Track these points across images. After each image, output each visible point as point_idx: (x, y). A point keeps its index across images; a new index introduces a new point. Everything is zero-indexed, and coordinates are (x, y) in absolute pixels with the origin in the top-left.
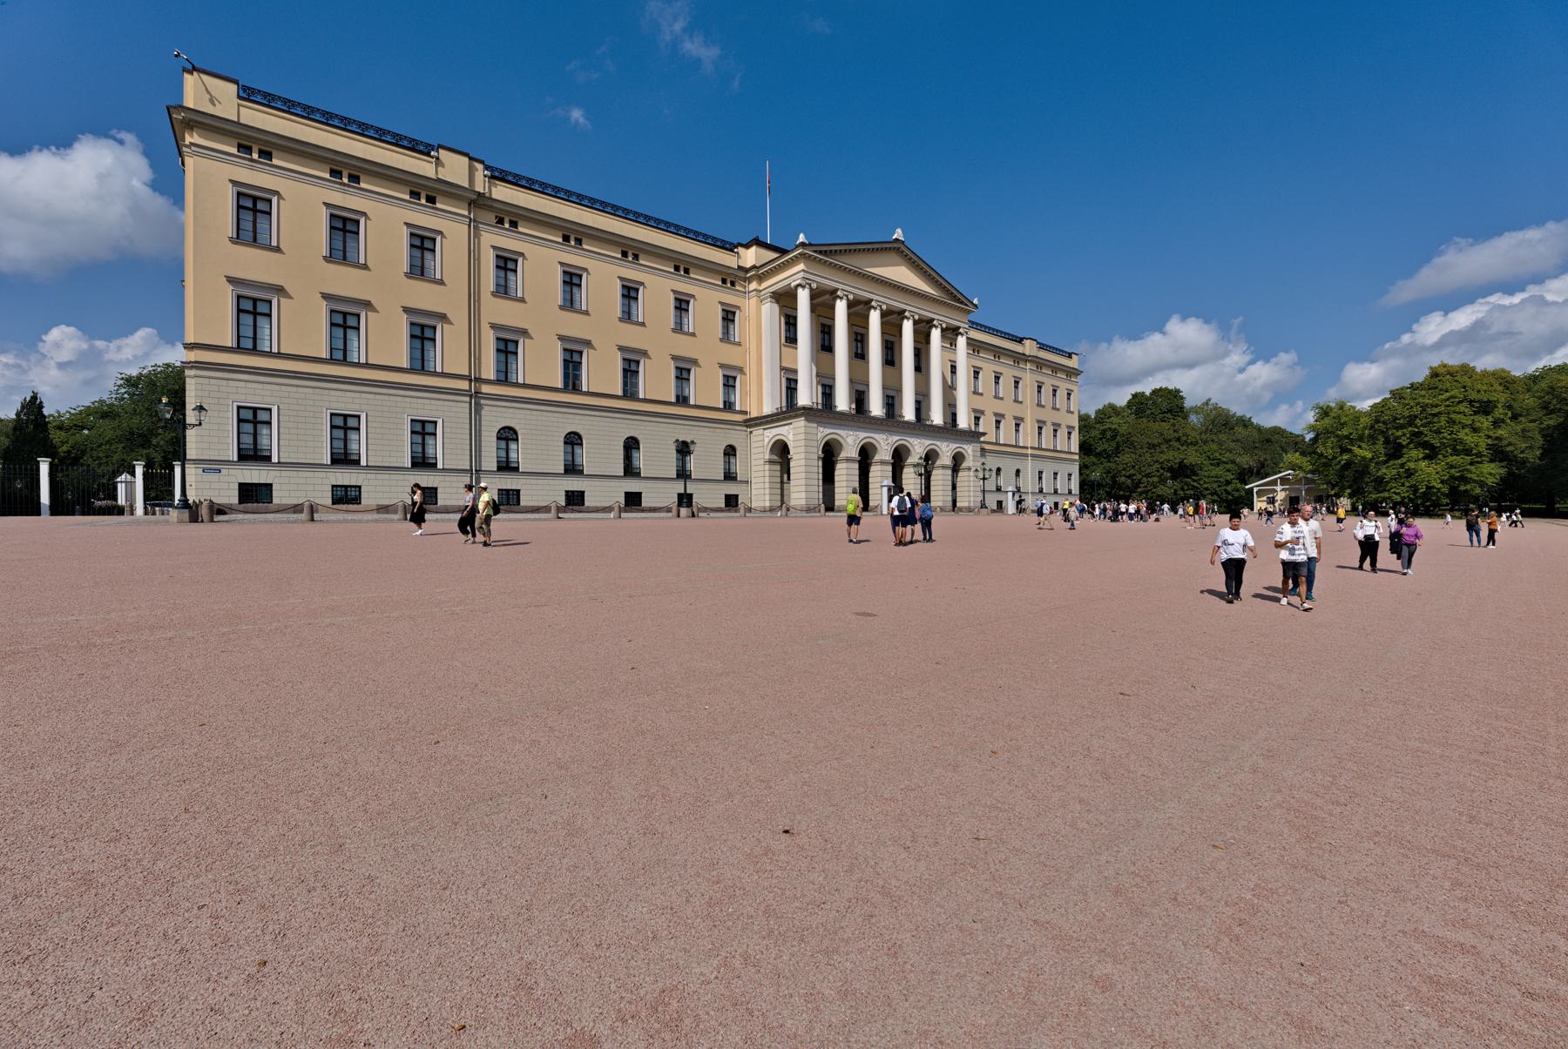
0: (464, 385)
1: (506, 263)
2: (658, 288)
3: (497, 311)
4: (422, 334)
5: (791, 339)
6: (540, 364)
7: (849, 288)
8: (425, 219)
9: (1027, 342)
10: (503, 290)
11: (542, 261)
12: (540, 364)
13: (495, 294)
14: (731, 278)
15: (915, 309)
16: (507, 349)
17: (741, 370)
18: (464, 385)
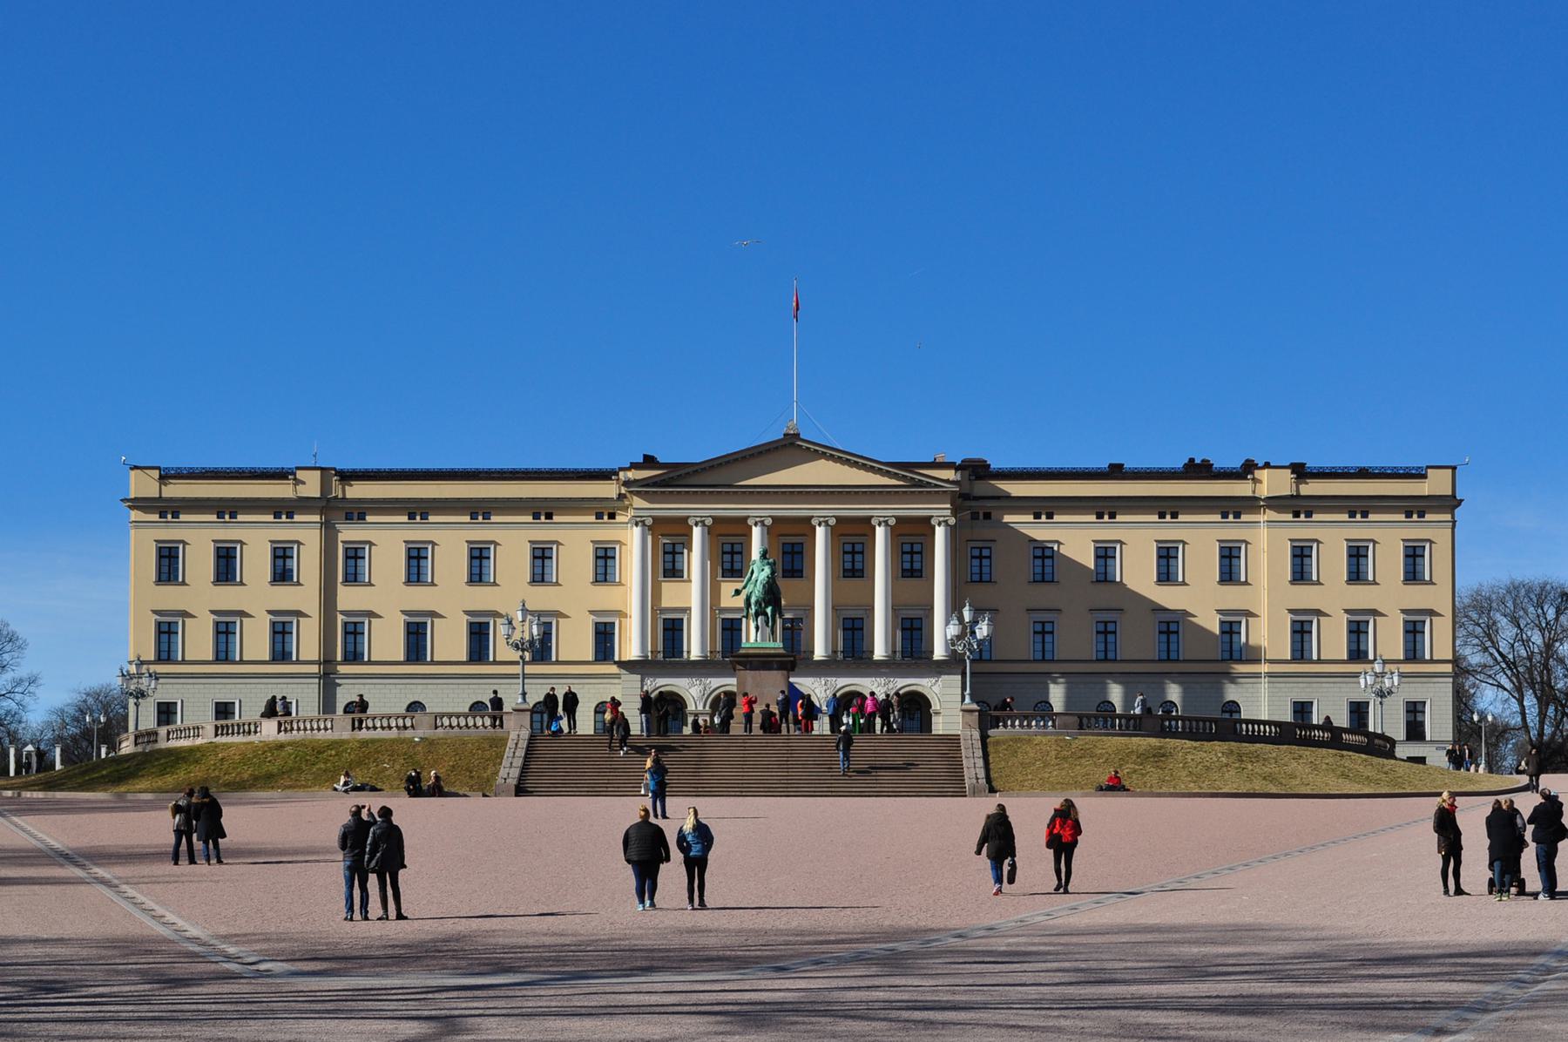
0: (314, 669)
1: (354, 554)
2: (512, 543)
3: (349, 598)
4: (281, 632)
5: (673, 571)
6: (386, 641)
7: (700, 512)
8: (284, 533)
9: (1263, 475)
10: (353, 578)
11: (386, 544)
12: (386, 641)
13: (346, 581)
14: (606, 511)
15: (823, 513)
16: (354, 632)
17: (621, 614)
18: (314, 669)
